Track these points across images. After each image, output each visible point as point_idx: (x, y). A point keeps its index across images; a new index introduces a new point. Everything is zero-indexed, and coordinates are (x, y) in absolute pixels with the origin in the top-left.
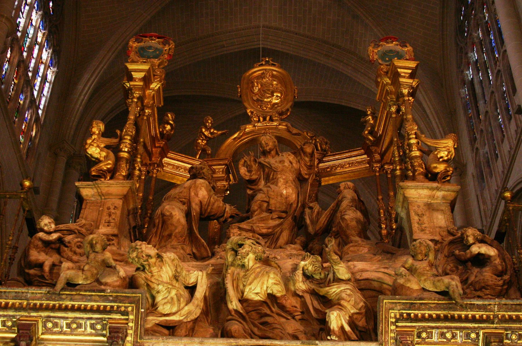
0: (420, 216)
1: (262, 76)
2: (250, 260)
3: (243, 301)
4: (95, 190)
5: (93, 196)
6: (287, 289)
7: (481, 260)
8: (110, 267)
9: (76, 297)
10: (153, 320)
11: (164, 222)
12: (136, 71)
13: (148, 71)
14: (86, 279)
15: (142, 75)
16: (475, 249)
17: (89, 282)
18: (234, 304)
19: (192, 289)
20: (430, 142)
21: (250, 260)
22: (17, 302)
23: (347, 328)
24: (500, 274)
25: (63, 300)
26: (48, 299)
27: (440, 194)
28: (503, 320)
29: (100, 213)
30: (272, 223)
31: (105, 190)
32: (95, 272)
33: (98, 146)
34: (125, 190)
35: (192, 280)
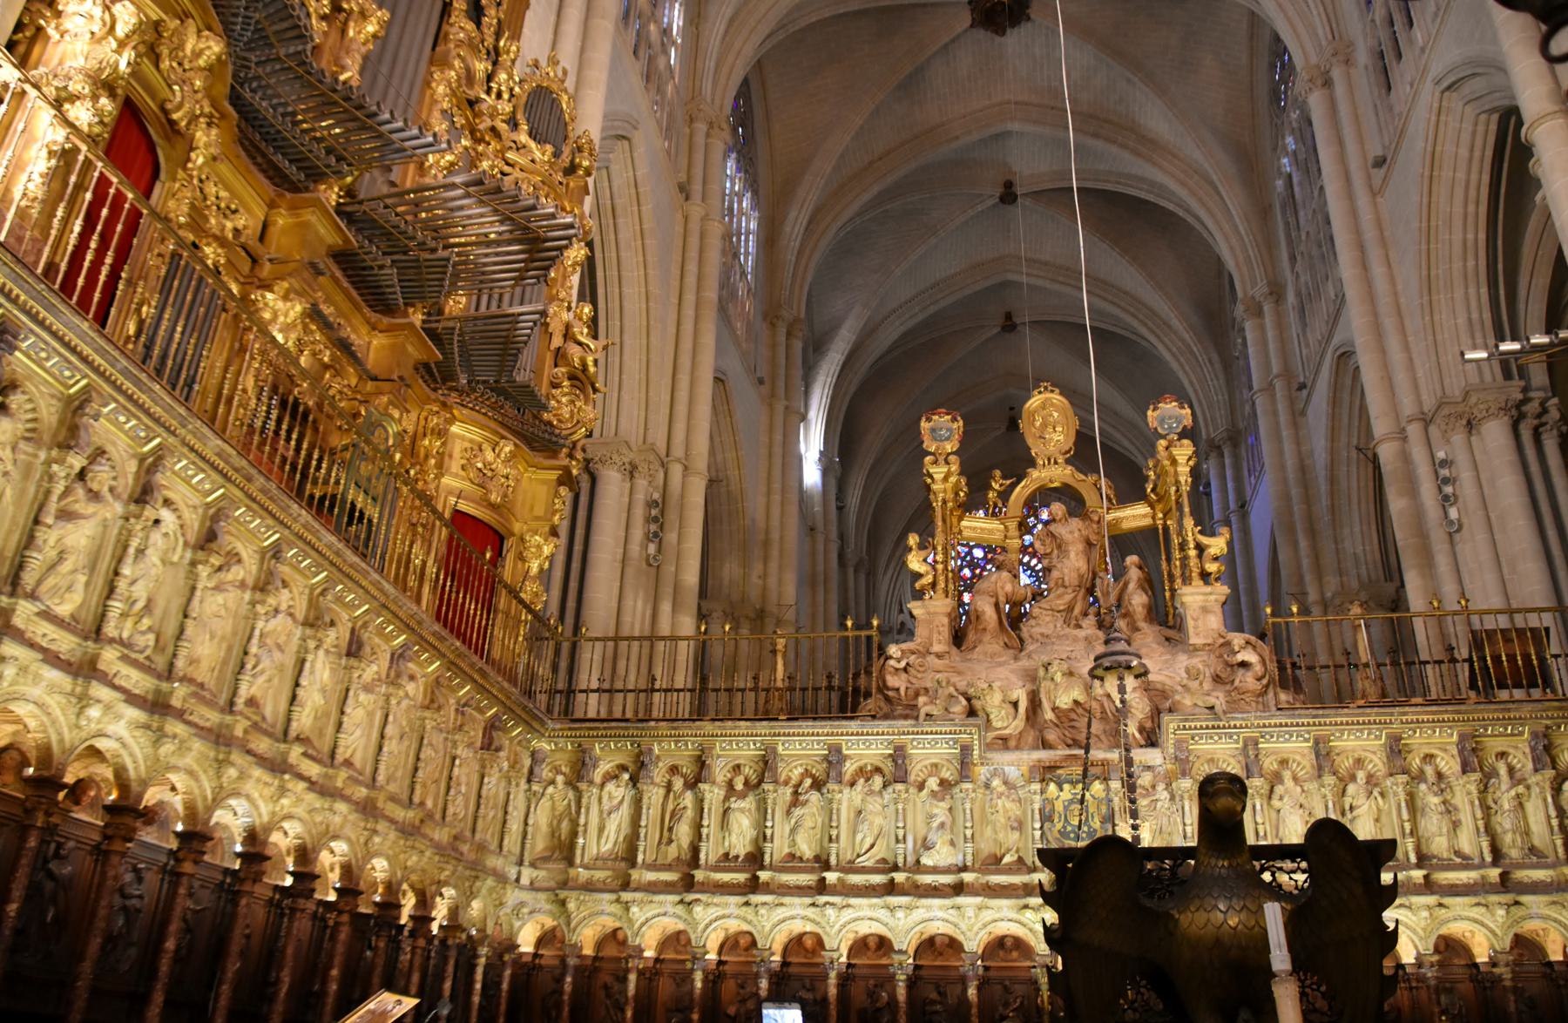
0: (1195, 620)
1: (1043, 406)
2: (1058, 677)
3: (1054, 709)
6: (1089, 694)
7: (1244, 665)
10: (991, 735)
11: (978, 618)
16: (1240, 657)
18: (1049, 715)
19: (1015, 704)
20: (1204, 540)
21: (1058, 677)
23: (1137, 735)
24: (1259, 679)
27: (1212, 598)
28: (1259, 726)
29: (931, 631)
30: (1068, 598)
35: (1014, 697)
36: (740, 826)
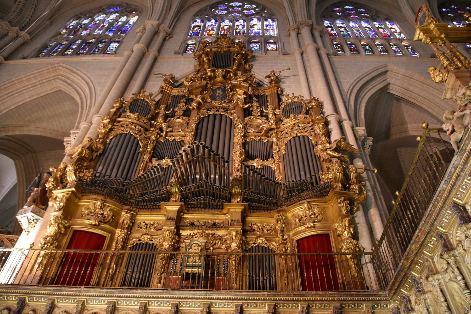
4: (449, 91)
5: (451, 93)
8: (464, 115)
9: (467, 142)
12: (419, 37)
13: (421, 30)
14: (460, 132)
15: (422, 34)
17: (463, 132)
22: (458, 169)
25: (466, 149)
26: (463, 156)
31: (450, 86)
32: (460, 126)
33: (437, 76)
34: (453, 77)
36: (453, 288)
